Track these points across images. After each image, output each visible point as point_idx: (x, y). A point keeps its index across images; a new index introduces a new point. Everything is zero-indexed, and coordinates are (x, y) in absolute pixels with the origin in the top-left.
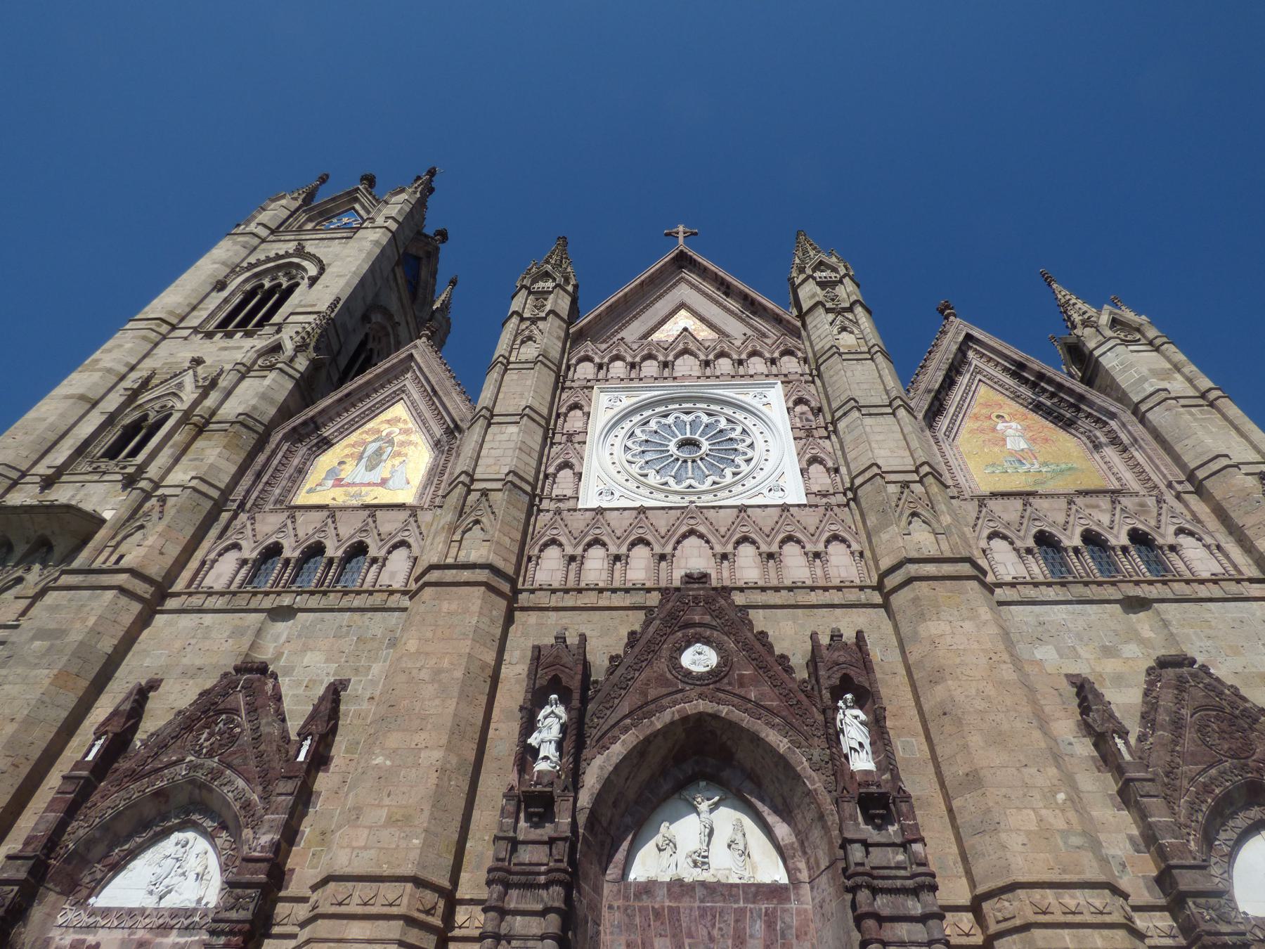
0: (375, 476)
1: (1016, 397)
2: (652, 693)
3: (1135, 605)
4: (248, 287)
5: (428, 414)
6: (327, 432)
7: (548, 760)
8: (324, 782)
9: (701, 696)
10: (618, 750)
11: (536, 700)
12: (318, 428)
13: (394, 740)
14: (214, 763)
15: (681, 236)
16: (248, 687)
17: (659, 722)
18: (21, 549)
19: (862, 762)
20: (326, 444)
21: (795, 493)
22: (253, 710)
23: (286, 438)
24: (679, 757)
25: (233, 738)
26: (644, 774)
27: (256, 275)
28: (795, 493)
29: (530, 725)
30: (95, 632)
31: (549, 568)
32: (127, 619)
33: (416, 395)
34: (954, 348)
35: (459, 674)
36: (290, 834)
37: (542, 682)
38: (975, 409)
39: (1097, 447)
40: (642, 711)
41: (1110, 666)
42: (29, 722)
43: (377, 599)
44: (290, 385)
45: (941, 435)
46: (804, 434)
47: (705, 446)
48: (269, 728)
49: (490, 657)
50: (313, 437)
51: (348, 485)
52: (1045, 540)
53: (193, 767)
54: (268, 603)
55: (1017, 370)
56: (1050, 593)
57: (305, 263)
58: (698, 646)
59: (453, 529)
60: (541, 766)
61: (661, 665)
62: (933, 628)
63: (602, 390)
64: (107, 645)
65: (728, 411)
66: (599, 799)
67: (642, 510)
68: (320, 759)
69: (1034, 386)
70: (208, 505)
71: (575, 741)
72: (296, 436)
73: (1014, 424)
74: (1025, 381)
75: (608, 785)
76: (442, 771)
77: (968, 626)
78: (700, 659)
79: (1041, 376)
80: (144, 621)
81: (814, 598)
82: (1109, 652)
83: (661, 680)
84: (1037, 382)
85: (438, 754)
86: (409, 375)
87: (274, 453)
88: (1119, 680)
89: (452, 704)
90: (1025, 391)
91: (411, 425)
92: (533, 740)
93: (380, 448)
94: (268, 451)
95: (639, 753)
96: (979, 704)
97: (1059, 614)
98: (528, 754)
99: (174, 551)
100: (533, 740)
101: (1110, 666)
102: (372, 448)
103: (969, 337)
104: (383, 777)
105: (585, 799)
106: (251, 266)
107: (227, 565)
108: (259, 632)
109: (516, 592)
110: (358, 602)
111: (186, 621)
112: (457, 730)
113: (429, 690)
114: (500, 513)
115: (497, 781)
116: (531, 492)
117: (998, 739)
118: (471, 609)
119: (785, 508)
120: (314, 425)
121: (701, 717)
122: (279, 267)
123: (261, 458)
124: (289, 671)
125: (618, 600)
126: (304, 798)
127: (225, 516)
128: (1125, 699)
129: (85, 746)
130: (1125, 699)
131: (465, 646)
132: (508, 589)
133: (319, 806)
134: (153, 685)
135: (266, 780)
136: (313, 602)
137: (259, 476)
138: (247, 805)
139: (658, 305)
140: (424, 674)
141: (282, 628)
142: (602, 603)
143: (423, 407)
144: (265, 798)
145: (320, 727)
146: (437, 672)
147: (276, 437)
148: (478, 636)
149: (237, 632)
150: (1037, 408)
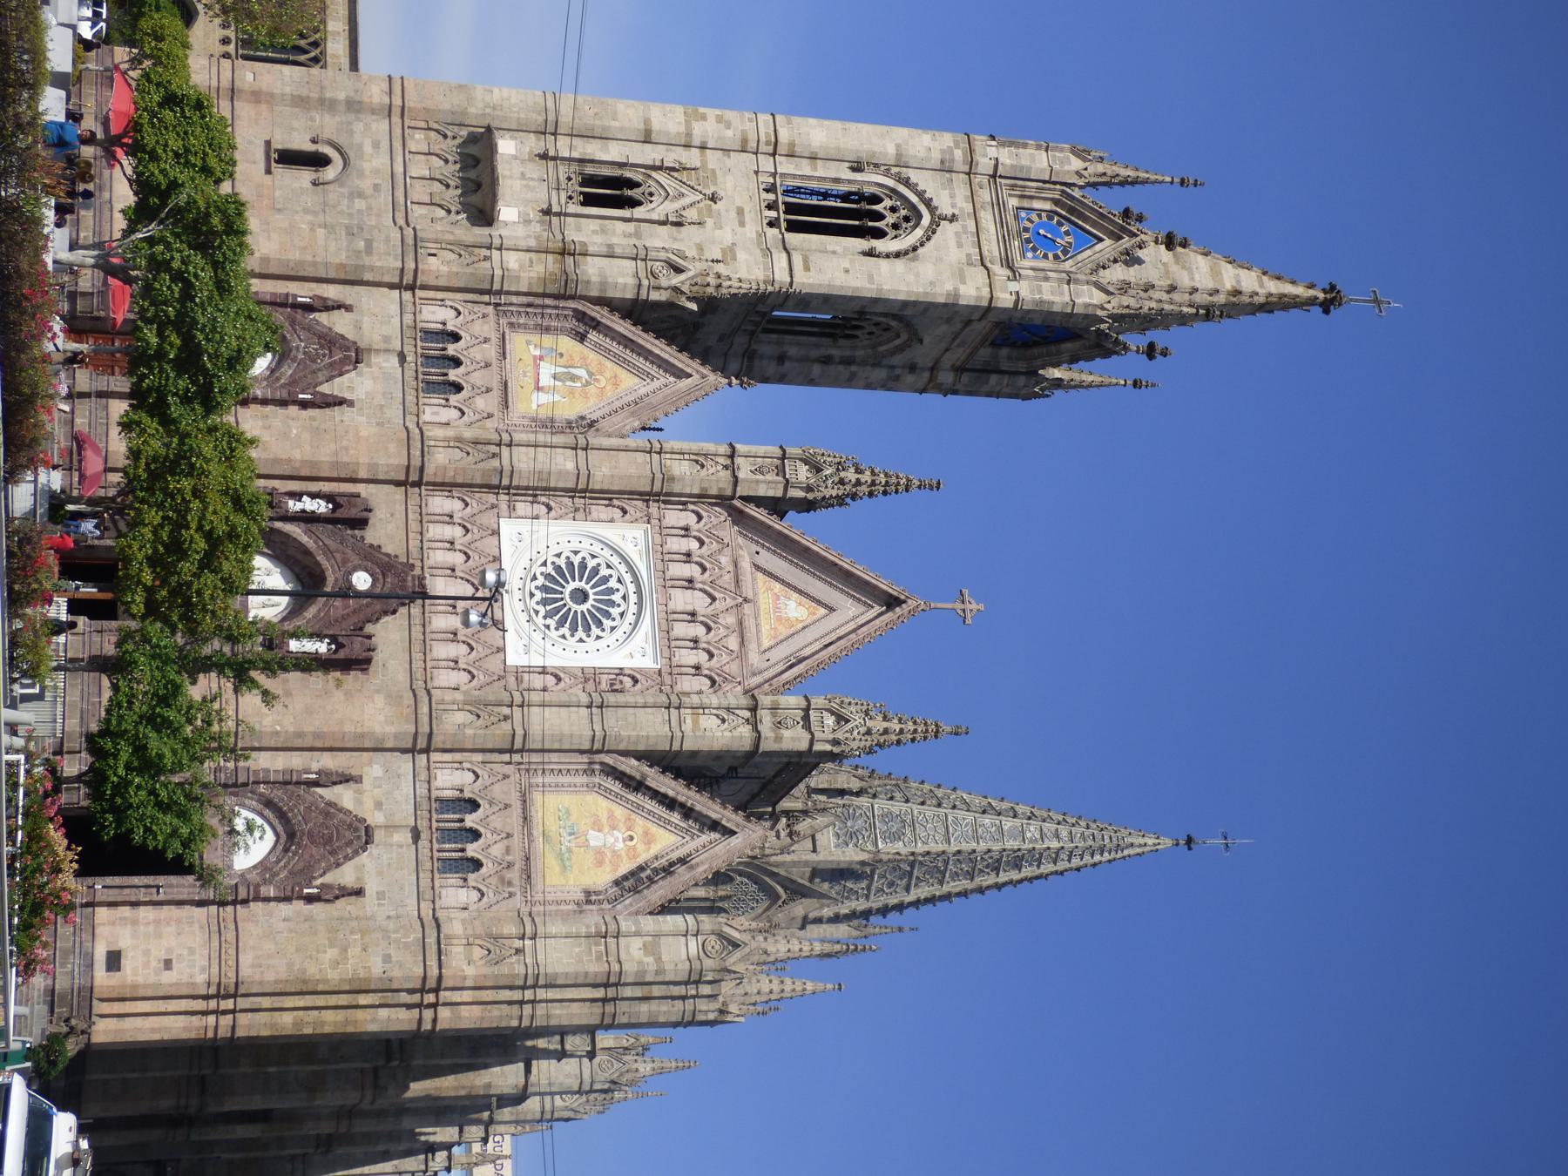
0: (545, 380)
1: (656, 858)
2: (338, 556)
3: (416, 836)
4: (868, 190)
5: (618, 404)
6: (593, 336)
7: (294, 506)
8: (293, 410)
9: (336, 580)
10: (304, 539)
11: (329, 498)
12: (594, 328)
13: (306, 436)
14: (301, 356)
15: (958, 606)
16: (347, 358)
17: (320, 558)
18: (472, 174)
19: (294, 645)
20: (582, 338)
21: (515, 657)
22: (331, 364)
23: (575, 310)
24: (311, 575)
25: (314, 361)
26: (299, 556)
27: (893, 191)
28: (515, 657)
29: (313, 496)
30: (372, 268)
31: (440, 503)
32: (387, 279)
33: (643, 391)
34: (714, 816)
35: (345, 459)
36: (264, 402)
37: (338, 499)
38: (639, 821)
39: (588, 893)
40: (328, 552)
41: (368, 803)
42: (314, 264)
43: (412, 408)
44: (629, 295)
45: (597, 780)
46: (589, 676)
47: (584, 607)
48: (321, 376)
49: (362, 474)
50: (583, 327)
51: (537, 367)
52: (474, 805)
53: (297, 348)
54: (409, 349)
55: (682, 861)
56: (422, 790)
57: (919, 232)
58: (370, 580)
59: (459, 439)
60: (291, 503)
61: (356, 560)
62: (380, 700)
63: (646, 531)
64: (368, 277)
65: (626, 627)
66: (279, 532)
67: (497, 559)
68: (304, 405)
69: (664, 869)
70: (486, 286)
71: (307, 518)
72: (581, 316)
73: (620, 845)
74: (672, 864)
75: (287, 536)
76: (290, 460)
77: (381, 718)
78: (362, 581)
79: (671, 873)
80: (392, 286)
81: (418, 656)
82: (379, 805)
83: (345, 561)
84: (668, 870)
85: (298, 457)
86: (672, 379)
87: (556, 307)
88: (359, 802)
89: (328, 459)
90: (663, 862)
91: (610, 393)
92: (305, 498)
93: (579, 378)
94: (556, 303)
95: (306, 552)
96: (329, 708)
97: (406, 787)
98: (297, 496)
99: (442, 282)
100: (305, 498)
101: (368, 803)
102: (582, 373)
103: (733, 833)
104: (285, 435)
105: (278, 525)
106: (906, 182)
107: (445, 314)
108: (387, 351)
109: (414, 484)
110: (411, 398)
111: (395, 308)
112: (314, 464)
113: (333, 446)
114: (481, 466)
115: (283, 486)
116: (506, 488)
117: (308, 711)
118: (392, 459)
119: (501, 650)
120: (596, 325)
121: (325, 579)
122: (913, 207)
123: (548, 301)
124: (359, 375)
125: (414, 543)
126: (283, 403)
127: (486, 298)
128: (344, 796)
129: (303, 292)
130: (344, 796)
131: (364, 460)
132: (412, 480)
133: (280, 411)
134: (348, 308)
135: (293, 382)
136: (410, 374)
137: (529, 305)
138: (278, 379)
139: (820, 584)
140: (345, 443)
141: (395, 360)
142: (411, 535)
143: (630, 398)
144: (283, 386)
145: (318, 400)
146: (346, 449)
147: (572, 304)
148: (373, 466)
149: (387, 339)
150: (641, 868)
